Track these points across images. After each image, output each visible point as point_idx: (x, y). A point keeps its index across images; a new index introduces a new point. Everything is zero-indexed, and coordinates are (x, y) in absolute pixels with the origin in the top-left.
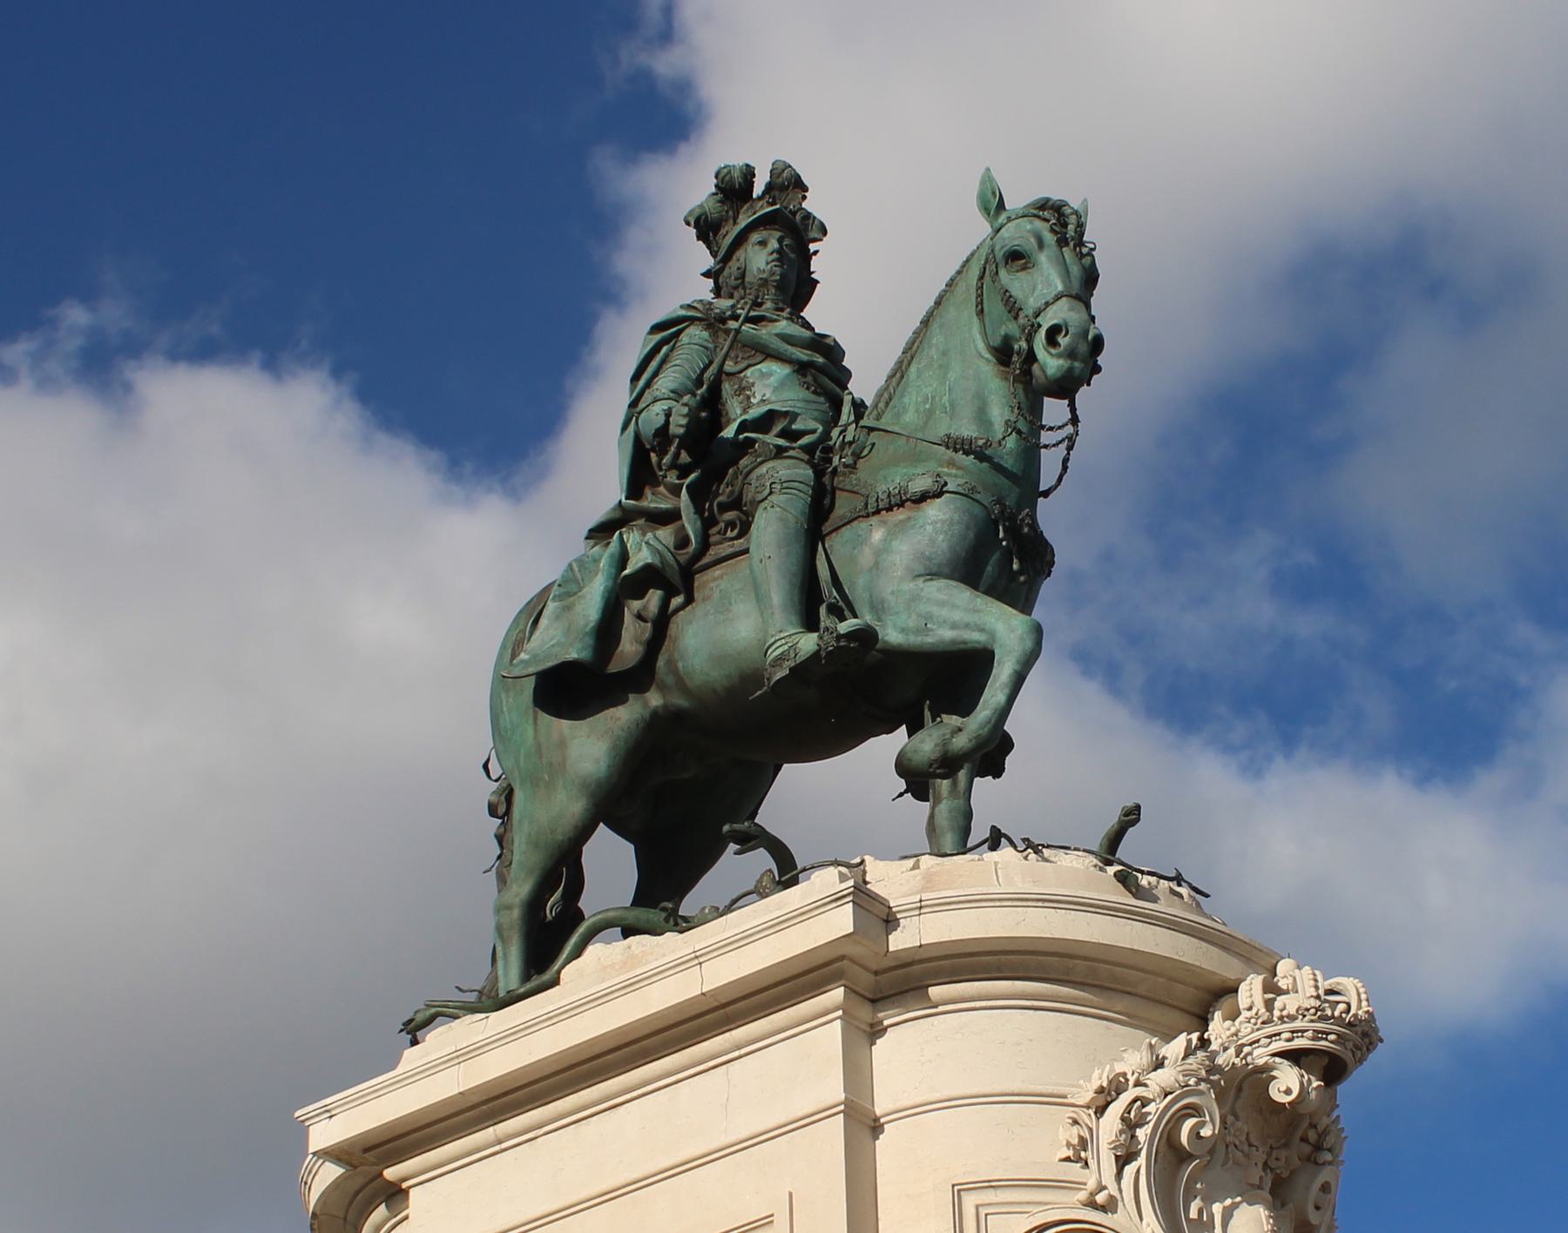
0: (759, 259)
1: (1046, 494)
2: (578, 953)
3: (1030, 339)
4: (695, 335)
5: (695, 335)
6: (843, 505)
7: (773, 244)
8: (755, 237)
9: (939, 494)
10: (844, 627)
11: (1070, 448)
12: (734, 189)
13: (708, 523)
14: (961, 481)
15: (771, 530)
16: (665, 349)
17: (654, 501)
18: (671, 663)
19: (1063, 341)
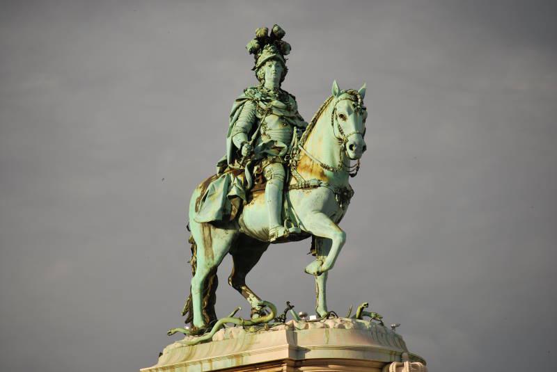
0: (269, 72)
1: (353, 176)
2: (218, 330)
3: (345, 145)
4: (249, 104)
5: (249, 104)
6: (293, 182)
7: (273, 67)
8: (268, 64)
9: (320, 186)
10: (291, 230)
11: (357, 170)
12: (262, 41)
13: (253, 177)
14: (325, 182)
15: (271, 186)
16: (240, 108)
17: (237, 166)
18: (243, 221)
19: (354, 148)
